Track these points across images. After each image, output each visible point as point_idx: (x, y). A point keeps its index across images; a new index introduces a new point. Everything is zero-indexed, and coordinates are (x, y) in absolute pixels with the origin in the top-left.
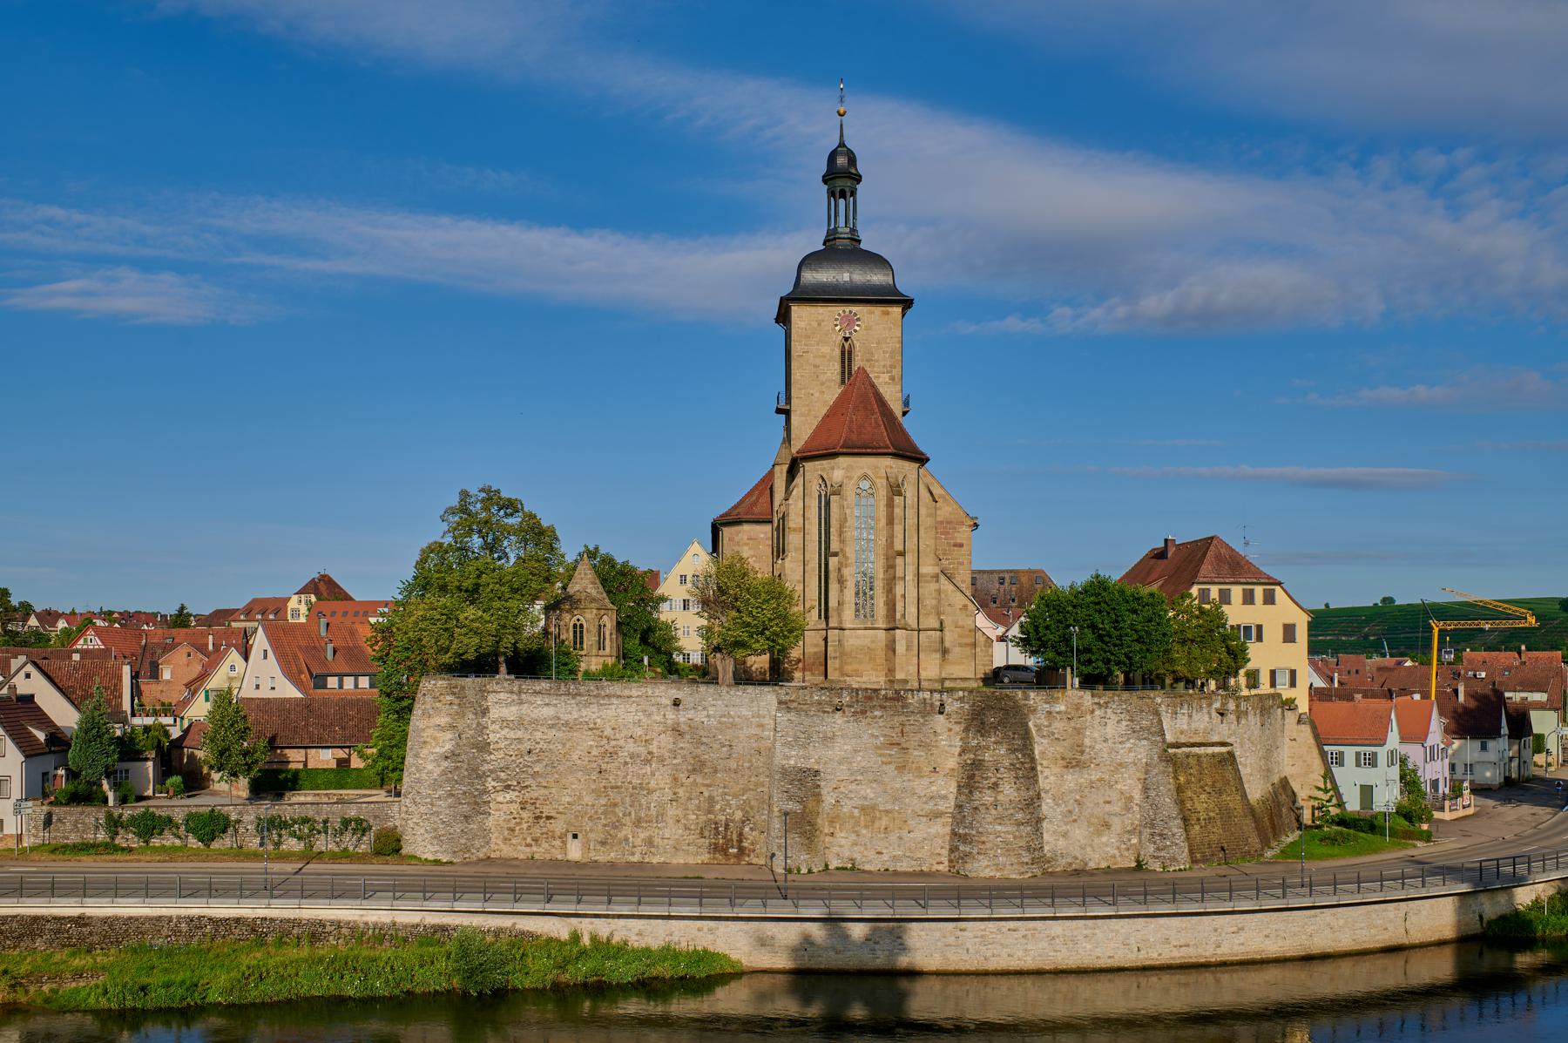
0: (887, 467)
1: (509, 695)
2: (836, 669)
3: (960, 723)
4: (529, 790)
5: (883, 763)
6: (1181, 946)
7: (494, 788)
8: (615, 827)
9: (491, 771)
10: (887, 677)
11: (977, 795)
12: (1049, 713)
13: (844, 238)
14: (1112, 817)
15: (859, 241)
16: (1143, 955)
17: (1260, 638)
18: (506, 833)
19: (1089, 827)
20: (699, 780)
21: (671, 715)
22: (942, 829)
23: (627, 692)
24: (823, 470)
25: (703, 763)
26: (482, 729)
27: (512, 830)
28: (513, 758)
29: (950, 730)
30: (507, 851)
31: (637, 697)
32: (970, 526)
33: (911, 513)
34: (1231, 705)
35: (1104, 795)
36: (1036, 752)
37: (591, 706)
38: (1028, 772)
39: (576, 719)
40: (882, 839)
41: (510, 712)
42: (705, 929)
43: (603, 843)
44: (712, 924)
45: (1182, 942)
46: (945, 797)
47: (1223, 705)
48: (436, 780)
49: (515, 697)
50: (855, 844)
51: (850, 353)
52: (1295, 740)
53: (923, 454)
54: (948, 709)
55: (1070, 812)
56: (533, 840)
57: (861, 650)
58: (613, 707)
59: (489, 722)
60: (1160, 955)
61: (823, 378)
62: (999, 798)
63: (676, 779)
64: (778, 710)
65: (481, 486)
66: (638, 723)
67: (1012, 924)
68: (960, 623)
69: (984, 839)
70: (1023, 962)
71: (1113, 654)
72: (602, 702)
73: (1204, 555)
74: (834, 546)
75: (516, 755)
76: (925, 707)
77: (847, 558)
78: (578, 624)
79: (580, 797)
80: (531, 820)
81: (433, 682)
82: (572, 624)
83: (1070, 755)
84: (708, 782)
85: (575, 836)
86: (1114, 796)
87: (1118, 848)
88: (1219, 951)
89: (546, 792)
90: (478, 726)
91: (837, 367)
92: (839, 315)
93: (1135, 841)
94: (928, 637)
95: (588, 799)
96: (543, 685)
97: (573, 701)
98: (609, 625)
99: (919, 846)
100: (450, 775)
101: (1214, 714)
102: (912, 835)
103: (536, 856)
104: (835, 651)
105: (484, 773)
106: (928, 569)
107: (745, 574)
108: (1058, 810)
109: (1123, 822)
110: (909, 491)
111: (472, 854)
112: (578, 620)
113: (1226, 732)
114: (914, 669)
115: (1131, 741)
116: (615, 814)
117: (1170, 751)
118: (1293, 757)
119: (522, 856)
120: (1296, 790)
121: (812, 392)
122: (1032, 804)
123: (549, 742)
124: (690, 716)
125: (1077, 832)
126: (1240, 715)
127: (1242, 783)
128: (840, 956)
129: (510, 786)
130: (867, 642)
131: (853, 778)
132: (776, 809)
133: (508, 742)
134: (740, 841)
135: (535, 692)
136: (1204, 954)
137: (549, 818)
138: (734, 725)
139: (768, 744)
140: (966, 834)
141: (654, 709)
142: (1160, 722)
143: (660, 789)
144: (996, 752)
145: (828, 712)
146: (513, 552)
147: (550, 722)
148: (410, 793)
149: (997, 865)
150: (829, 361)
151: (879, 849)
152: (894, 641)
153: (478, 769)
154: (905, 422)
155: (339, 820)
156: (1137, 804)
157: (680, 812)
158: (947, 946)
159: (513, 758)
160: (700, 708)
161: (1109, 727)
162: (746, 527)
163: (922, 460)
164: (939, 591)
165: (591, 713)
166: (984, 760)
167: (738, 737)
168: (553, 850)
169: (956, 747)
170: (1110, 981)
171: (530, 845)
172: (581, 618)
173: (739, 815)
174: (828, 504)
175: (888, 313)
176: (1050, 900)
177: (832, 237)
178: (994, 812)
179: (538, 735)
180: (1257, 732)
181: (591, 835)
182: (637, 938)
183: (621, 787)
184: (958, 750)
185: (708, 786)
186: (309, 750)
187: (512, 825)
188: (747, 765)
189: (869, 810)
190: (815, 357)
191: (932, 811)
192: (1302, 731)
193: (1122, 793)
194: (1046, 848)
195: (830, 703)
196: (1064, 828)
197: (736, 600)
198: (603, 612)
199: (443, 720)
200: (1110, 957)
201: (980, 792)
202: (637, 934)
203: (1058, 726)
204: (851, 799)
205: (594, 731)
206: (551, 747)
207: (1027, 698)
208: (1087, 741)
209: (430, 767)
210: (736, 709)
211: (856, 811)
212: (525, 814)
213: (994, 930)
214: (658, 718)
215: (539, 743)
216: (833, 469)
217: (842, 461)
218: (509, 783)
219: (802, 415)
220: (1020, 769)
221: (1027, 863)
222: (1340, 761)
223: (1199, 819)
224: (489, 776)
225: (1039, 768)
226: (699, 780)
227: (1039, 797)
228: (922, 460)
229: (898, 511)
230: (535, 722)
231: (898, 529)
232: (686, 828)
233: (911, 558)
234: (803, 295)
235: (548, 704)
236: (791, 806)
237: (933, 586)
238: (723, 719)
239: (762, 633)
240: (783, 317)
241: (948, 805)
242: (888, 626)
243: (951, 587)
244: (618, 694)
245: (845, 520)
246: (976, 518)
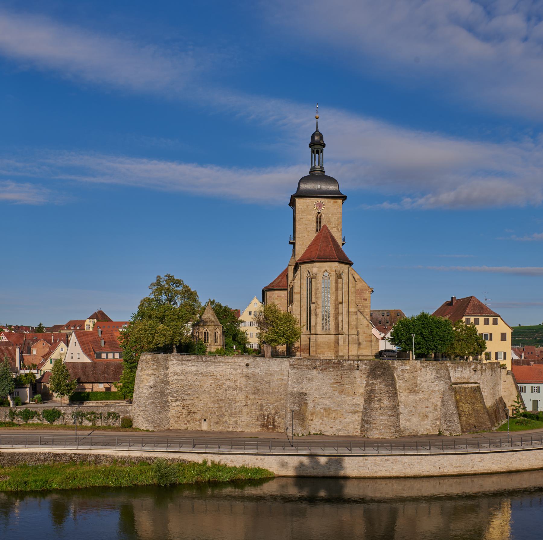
0: (335, 267)
1: (177, 361)
2: (314, 351)
3: (365, 374)
4: (186, 401)
6: (457, 467)
7: (171, 400)
8: (222, 417)
9: (170, 393)
10: (335, 354)
12: (403, 370)
13: (318, 171)
14: (429, 413)
15: (324, 172)
16: (441, 470)
17: (491, 339)
18: (176, 419)
19: (419, 417)
20: (257, 397)
21: (245, 370)
22: (357, 418)
23: (226, 361)
24: (309, 268)
25: (258, 390)
26: (166, 375)
27: (179, 418)
28: (179, 388)
29: (361, 377)
30: (177, 426)
31: (231, 362)
32: (370, 292)
33: (345, 286)
34: (479, 367)
35: (425, 404)
36: (397, 386)
37: (212, 366)
38: (394, 394)
39: (205, 372)
40: (333, 422)
41: (178, 369)
42: (259, 459)
43: (217, 423)
44: (262, 457)
45: (458, 465)
46: (359, 405)
47: (475, 367)
48: (147, 397)
49: (180, 362)
50: (321, 424)
51: (320, 219)
52: (505, 381)
53: (351, 261)
54: (360, 368)
55: (411, 411)
56: (187, 422)
57: (324, 343)
58: (221, 366)
59: (169, 373)
60: (448, 470)
62: (381, 405)
64: (290, 368)
65: (166, 275)
66: (231, 373)
67: (387, 458)
68: (366, 332)
69: (375, 422)
70: (391, 473)
71: (430, 345)
72: (216, 364)
73: (468, 304)
74: (313, 300)
75: (180, 387)
76: (351, 367)
77: (318, 305)
78: (206, 332)
79: (207, 404)
80: (186, 413)
81: (146, 356)
82: (203, 332)
83: (411, 387)
84: (260, 398)
85: (205, 420)
86: (430, 405)
87: (431, 426)
88: (473, 469)
89: (193, 402)
90: (164, 374)
92: (316, 203)
93: (438, 423)
94: (352, 338)
95: (210, 405)
96: (192, 357)
97: (204, 364)
98: (219, 333)
99: (348, 425)
100: (153, 395)
101: (472, 371)
102: (345, 420)
103: (189, 429)
104: (313, 344)
105: (167, 394)
106: (352, 310)
107: (276, 312)
108: (406, 410)
109: (433, 415)
110: (345, 277)
111: (162, 427)
112: (206, 330)
113: (477, 378)
114: (346, 351)
115: (437, 382)
116: (222, 411)
117: (453, 386)
118: (505, 389)
119: (183, 429)
120: (506, 402)
121: (304, 235)
122: (395, 408)
123: (194, 381)
124: (253, 371)
125: (414, 419)
126: (482, 371)
127: (483, 400)
128: (315, 470)
129: (178, 399)
130: (327, 340)
131: (321, 396)
132: (289, 409)
133: (177, 381)
134: (274, 422)
135: (188, 360)
136: (467, 470)
137: (194, 413)
138: (271, 374)
139: (285, 382)
140: (368, 420)
141: (238, 367)
142: (449, 374)
143: (240, 401)
144: (380, 386)
145: (310, 369)
146: (179, 301)
147: (194, 373)
148: (136, 402)
149: (381, 433)
150: (312, 222)
151: (332, 426)
152: (338, 339)
153: (164, 392)
154: (343, 248)
155: (107, 413)
156: (439, 408)
157: (249, 411)
158: (359, 466)
159: (179, 388)
160: (257, 367)
161: (427, 376)
162: (276, 292)
163: (350, 264)
164: (357, 319)
165: (212, 369)
166: (375, 389)
167: (273, 379)
168: (196, 426)
169: (364, 384)
170: (428, 481)
171: (187, 424)
172: (208, 329)
173: (273, 412)
174: (311, 282)
175: (336, 202)
176: (364, 448)
177: (313, 170)
178: (379, 411)
179: (190, 378)
180: (489, 378)
181: (212, 420)
182: (230, 463)
183: (224, 400)
184: (365, 385)
185: (260, 399)
186: (94, 384)
187: (178, 416)
188: (276, 391)
189: (327, 410)
191: (353, 410)
192: (508, 378)
193: (433, 403)
194: (401, 426)
195: (311, 365)
196: (409, 418)
197: (272, 322)
198: (216, 327)
199: (150, 372)
200: (428, 471)
201: (374, 403)
202: (231, 461)
203: (406, 375)
204: (320, 405)
205: (213, 377)
206: (195, 383)
207: (393, 364)
208: (418, 382)
209: (145, 391)
210: (272, 368)
211: (322, 410)
212: (184, 411)
213: (380, 460)
214: (240, 371)
215: (190, 381)
216: (313, 267)
217: (317, 264)
218: (178, 398)
219: (300, 245)
220: (390, 393)
221: (393, 432)
222: (524, 390)
223: (465, 414)
224: (169, 395)
225: (398, 393)
226: (257, 397)
227: (398, 405)
228: (350, 264)
229: (340, 285)
230: (188, 373)
231: (340, 293)
232: (251, 417)
234: (301, 194)
235: (193, 365)
236: (295, 408)
237: (355, 317)
239: (283, 336)
240: (292, 204)
241: (360, 408)
242: (336, 333)
243: (362, 317)
244: (223, 361)
245: (318, 289)
246: (373, 288)
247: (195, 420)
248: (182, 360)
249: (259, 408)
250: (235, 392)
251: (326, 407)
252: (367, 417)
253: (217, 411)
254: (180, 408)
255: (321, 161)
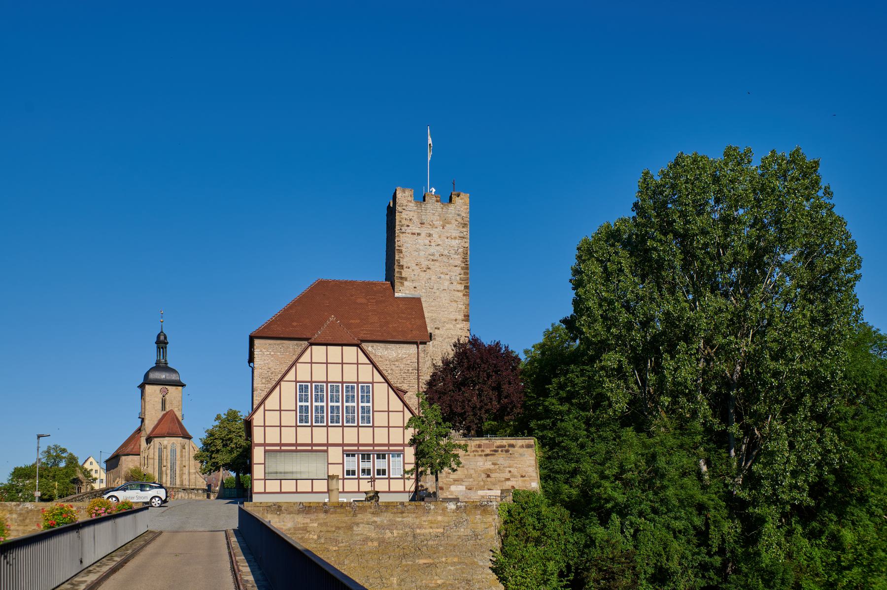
33: (187, 454)
61: (156, 408)
91: (161, 405)
154: (184, 423)
163: (189, 438)
228: (189, 438)
229: (184, 454)
231: (184, 459)
233: (187, 467)
234: (147, 381)
237: (194, 476)
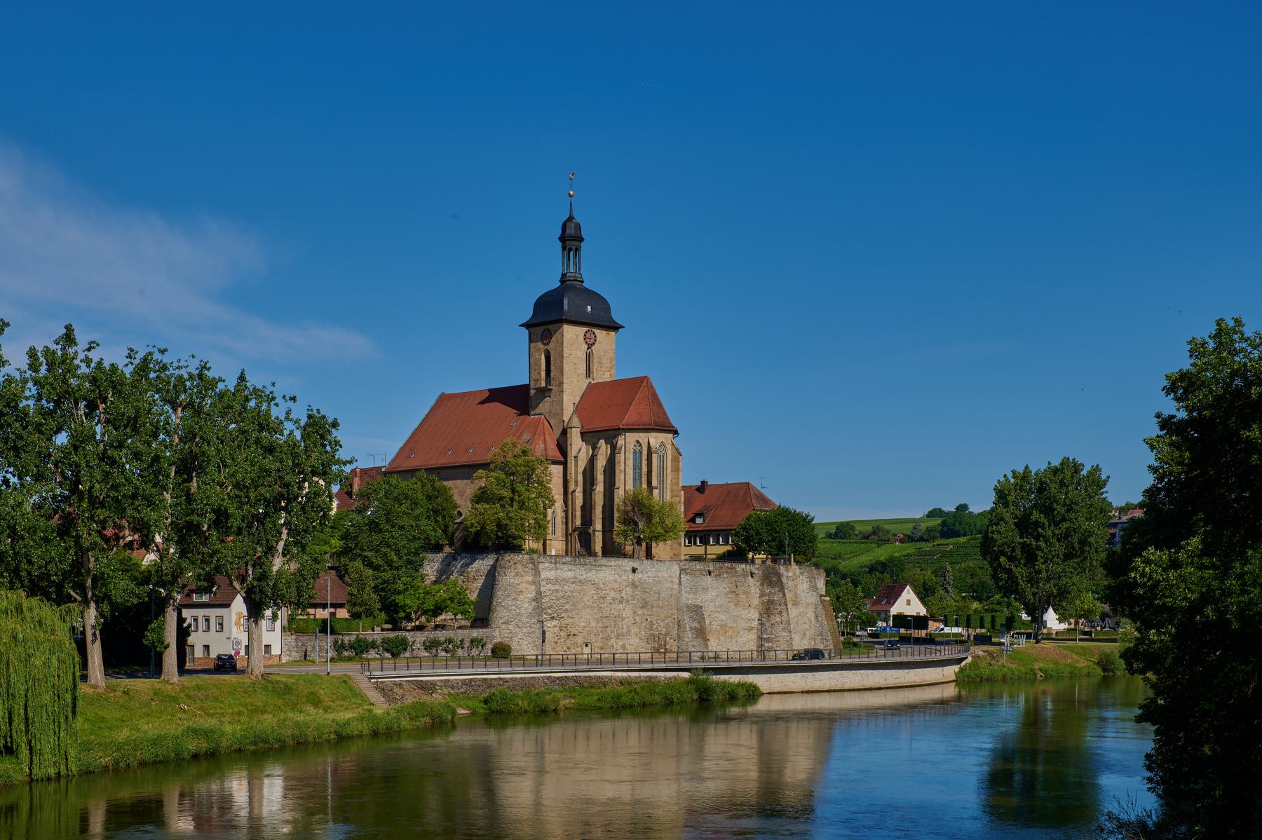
5: (729, 602)
8: (607, 640)
11: (773, 617)
20: (646, 612)
21: (631, 576)
22: (753, 636)
23: (609, 564)
24: (640, 437)
25: (647, 603)
39: (585, 579)
48: (530, 613)
61: (578, 372)
63: (635, 612)
66: (615, 581)
71: (799, 547)
79: (589, 623)
85: (587, 645)
95: (593, 624)
116: (607, 632)
134: (665, 645)
137: (574, 635)
141: (623, 572)
148: (512, 622)
157: (637, 630)
163: (675, 432)
165: (592, 575)
175: (609, 334)
178: (781, 626)
179: (566, 588)
181: (596, 644)
185: (650, 615)
187: (556, 640)
188: (667, 603)
189: (723, 627)
190: (575, 358)
195: (704, 570)
199: (530, 578)
206: (574, 594)
209: (527, 606)
212: (562, 634)
214: (625, 578)
226: (646, 612)
228: (675, 432)
230: (564, 580)
235: (571, 570)
236: (695, 625)
238: (655, 579)
244: (605, 564)
247: (575, 644)
248: (556, 563)
249: (649, 626)
250: (621, 607)
251: (723, 623)
252: (767, 634)
253: (602, 631)
254: (557, 629)
255: (578, 266)
